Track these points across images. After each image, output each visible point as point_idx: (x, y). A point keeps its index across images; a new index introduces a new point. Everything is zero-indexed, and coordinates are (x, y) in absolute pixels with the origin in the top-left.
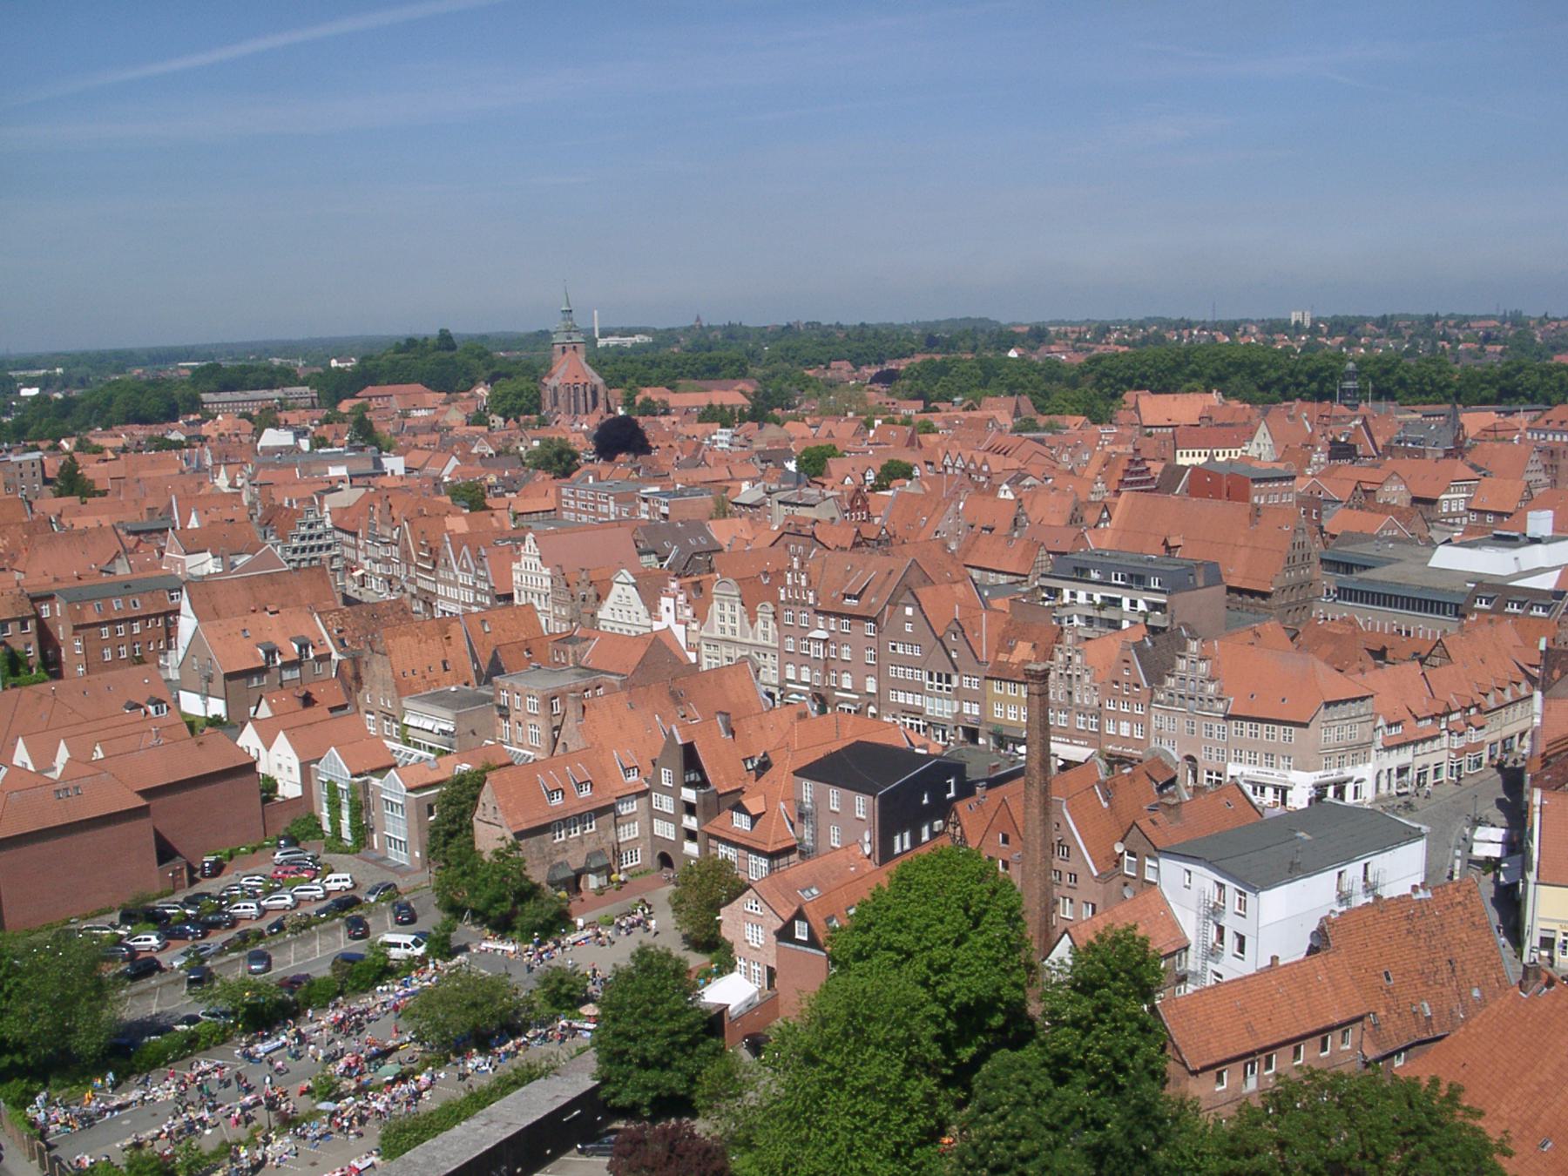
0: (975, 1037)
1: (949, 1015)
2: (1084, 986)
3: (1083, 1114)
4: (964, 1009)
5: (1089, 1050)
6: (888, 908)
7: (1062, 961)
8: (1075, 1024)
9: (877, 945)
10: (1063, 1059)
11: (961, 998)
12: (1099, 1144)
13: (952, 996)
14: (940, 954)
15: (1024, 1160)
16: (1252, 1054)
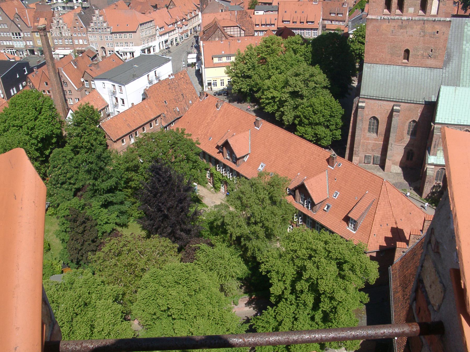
0: (48, 146)
1: (39, 142)
2: (78, 124)
3: (86, 161)
4: (42, 139)
5: (83, 142)
6: (10, 113)
7: (69, 118)
8: (78, 136)
9: (9, 126)
10: (76, 147)
11: (40, 136)
12: (88, 169)
13: (37, 136)
14: (30, 124)
15: (70, 179)
16: (131, 132)
